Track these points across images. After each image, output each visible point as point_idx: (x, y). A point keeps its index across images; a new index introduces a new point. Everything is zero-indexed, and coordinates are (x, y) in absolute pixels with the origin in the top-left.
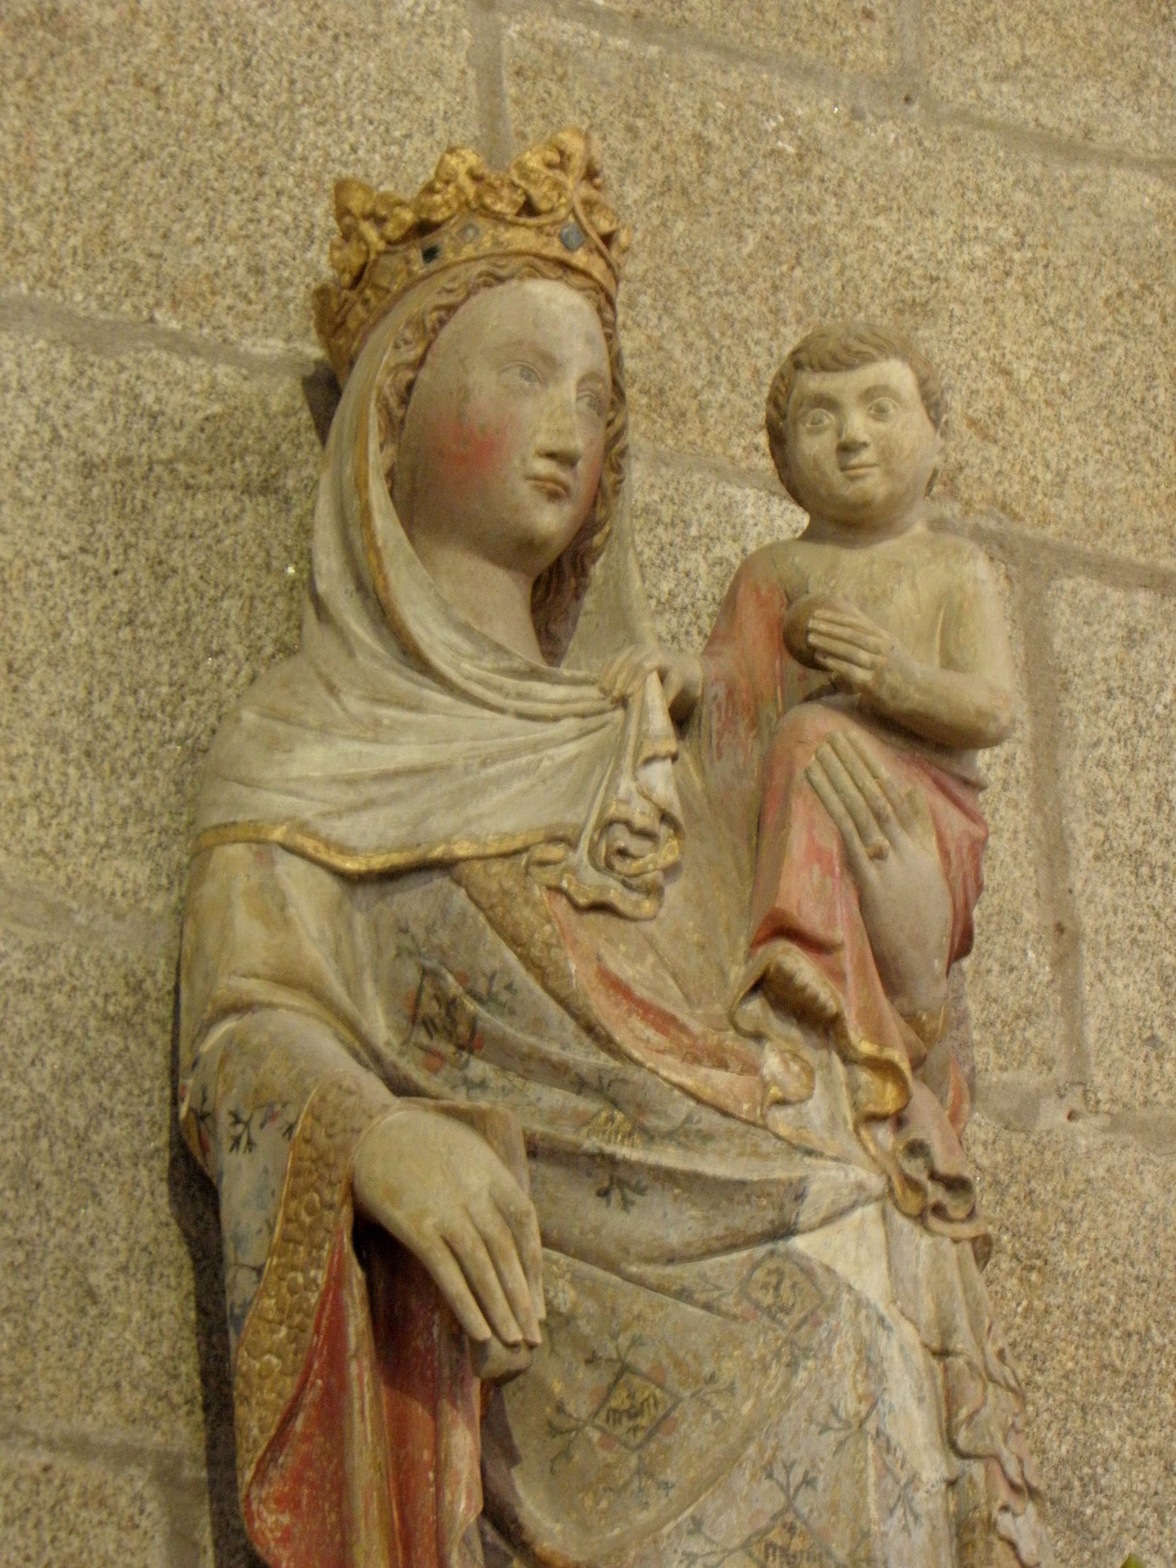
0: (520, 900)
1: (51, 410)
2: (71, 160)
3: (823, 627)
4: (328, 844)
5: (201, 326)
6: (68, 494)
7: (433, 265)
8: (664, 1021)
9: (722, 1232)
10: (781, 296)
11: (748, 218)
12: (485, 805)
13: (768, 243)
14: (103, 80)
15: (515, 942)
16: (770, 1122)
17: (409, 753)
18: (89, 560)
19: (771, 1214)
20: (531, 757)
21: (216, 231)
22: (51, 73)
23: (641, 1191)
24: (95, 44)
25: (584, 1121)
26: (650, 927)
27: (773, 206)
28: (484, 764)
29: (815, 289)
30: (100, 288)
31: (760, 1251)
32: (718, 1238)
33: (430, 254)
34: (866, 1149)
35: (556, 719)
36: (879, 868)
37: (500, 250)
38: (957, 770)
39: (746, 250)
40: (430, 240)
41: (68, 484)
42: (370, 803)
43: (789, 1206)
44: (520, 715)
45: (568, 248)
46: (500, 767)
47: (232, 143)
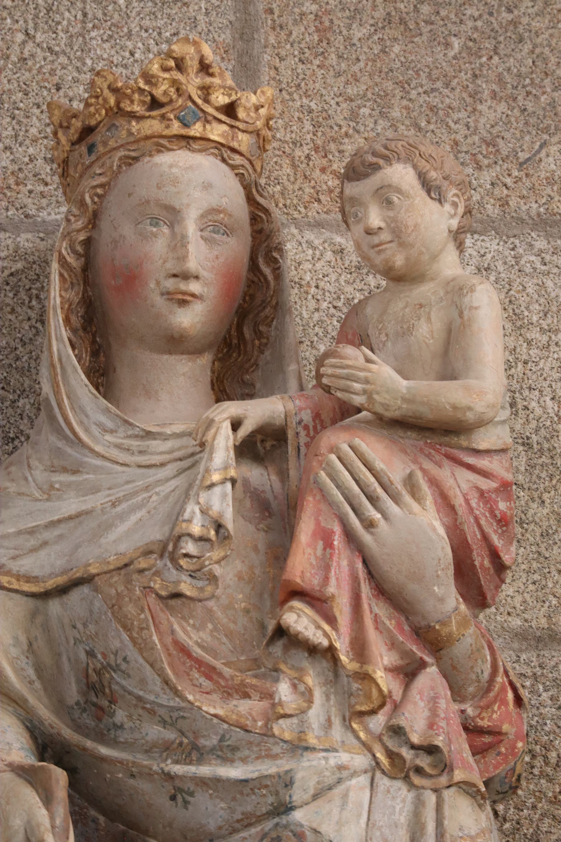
0: (127, 599)
3: (330, 371)
4: (18, 577)
5: (7, 210)
7: (93, 157)
8: (210, 672)
9: (240, 817)
10: (479, 82)
11: (454, 29)
12: (112, 536)
13: (471, 44)
15: (127, 628)
16: (276, 731)
17: (71, 505)
19: (271, 799)
20: (146, 495)
21: (20, 139)
23: (192, 794)
25: (167, 748)
26: (211, 604)
27: (476, 14)
28: (114, 505)
29: (509, 69)
31: (269, 825)
32: (238, 821)
33: (91, 149)
34: (358, 738)
35: (162, 465)
36: (372, 534)
37: (132, 139)
38: (464, 443)
39: (451, 54)
40: (90, 139)
42: (45, 544)
43: (282, 792)
46: (124, 505)
47: (35, 72)
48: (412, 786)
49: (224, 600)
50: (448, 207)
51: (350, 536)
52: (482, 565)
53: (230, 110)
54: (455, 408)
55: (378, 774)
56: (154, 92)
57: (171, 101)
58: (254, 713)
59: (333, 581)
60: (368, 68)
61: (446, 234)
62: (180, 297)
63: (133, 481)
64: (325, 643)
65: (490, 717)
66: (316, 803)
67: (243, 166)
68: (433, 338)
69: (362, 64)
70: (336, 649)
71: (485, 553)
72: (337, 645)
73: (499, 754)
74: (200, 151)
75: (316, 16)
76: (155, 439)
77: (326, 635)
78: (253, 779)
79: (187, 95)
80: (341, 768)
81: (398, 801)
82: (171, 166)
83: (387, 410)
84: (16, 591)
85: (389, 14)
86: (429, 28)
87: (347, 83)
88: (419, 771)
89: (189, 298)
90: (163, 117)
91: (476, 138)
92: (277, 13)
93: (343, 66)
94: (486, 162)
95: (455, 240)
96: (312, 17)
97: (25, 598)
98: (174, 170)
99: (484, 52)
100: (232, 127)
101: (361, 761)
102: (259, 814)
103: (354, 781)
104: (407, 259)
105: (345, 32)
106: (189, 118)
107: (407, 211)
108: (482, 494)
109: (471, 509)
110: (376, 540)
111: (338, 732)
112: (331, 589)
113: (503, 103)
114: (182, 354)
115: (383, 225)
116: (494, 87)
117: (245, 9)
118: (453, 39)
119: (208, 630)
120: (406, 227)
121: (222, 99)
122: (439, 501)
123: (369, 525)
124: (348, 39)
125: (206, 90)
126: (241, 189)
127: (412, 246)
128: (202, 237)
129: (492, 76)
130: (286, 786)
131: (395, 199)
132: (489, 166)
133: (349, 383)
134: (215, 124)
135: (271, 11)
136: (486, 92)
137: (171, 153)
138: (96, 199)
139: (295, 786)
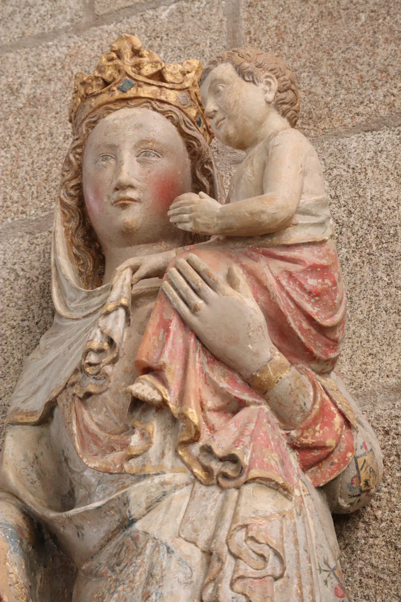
1: (16, 267)
2: (35, 156)
4: (27, 414)
6: (19, 299)
10: (377, 35)
11: (361, 8)
13: (372, 14)
14: (54, 114)
18: (26, 323)
19: (117, 517)
22: (31, 123)
24: (52, 100)
28: (69, 348)
30: (42, 204)
36: (197, 315)
39: (360, 23)
41: (20, 295)
43: (123, 509)
44: (84, 317)
45: (124, 92)
48: (222, 489)
49: (113, 390)
50: (262, 86)
51: (184, 322)
52: (301, 328)
53: (160, 76)
54: (252, 214)
55: (197, 484)
56: (104, 77)
57: (114, 79)
58: (115, 460)
59: (166, 354)
60: (307, 48)
61: (264, 104)
62: (121, 202)
63: (81, 328)
64: (158, 398)
65: (313, 437)
66: (150, 514)
67: (170, 111)
68: (254, 175)
69: (303, 47)
70: (167, 401)
71: (301, 318)
72: (168, 398)
73: (333, 464)
74: (135, 106)
75: (277, 27)
76: (94, 297)
77: (160, 393)
78: (104, 505)
79: (123, 73)
80: (163, 484)
81: (211, 500)
82: (114, 120)
83: (209, 228)
84: (26, 424)
85: (321, 12)
86: (346, 12)
87: (294, 60)
88: (225, 476)
89: (127, 202)
90: (109, 90)
91: (374, 71)
92: (253, 32)
93: (292, 51)
94: (380, 83)
95: (278, 110)
96: (274, 28)
97: (34, 428)
98: (116, 122)
99: (380, 17)
100: (160, 87)
101: (182, 477)
102: (112, 530)
103: (177, 493)
104: (236, 127)
105: (293, 31)
106: (126, 87)
107: (229, 93)
108: (290, 275)
109: (282, 287)
110: (200, 320)
111: (169, 460)
112: (165, 359)
113: (393, 44)
114: (139, 244)
115: (216, 108)
116: (387, 35)
117: (233, 36)
118: (361, 14)
119: (103, 413)
120: (229, 105)
121: (148, 69)
122: (256, 285)
123: (194, 310)
124: (296, 35)
125: (138, 66)
126: (174, 127)
127: (236, 117)
128: (137, 161)
129: (385, 29)
130: (125, 504)
131: (221, 88)
132: (383, 85)
133: (181, 215)
134: (145, 87)
135: (249, 33)
136: (381, 40)
137: (117, 112)
138: (77, 156)
139: (131, 503)
